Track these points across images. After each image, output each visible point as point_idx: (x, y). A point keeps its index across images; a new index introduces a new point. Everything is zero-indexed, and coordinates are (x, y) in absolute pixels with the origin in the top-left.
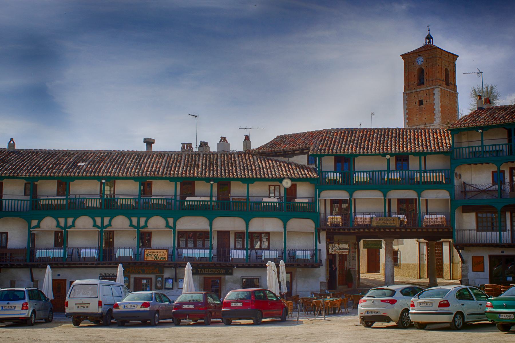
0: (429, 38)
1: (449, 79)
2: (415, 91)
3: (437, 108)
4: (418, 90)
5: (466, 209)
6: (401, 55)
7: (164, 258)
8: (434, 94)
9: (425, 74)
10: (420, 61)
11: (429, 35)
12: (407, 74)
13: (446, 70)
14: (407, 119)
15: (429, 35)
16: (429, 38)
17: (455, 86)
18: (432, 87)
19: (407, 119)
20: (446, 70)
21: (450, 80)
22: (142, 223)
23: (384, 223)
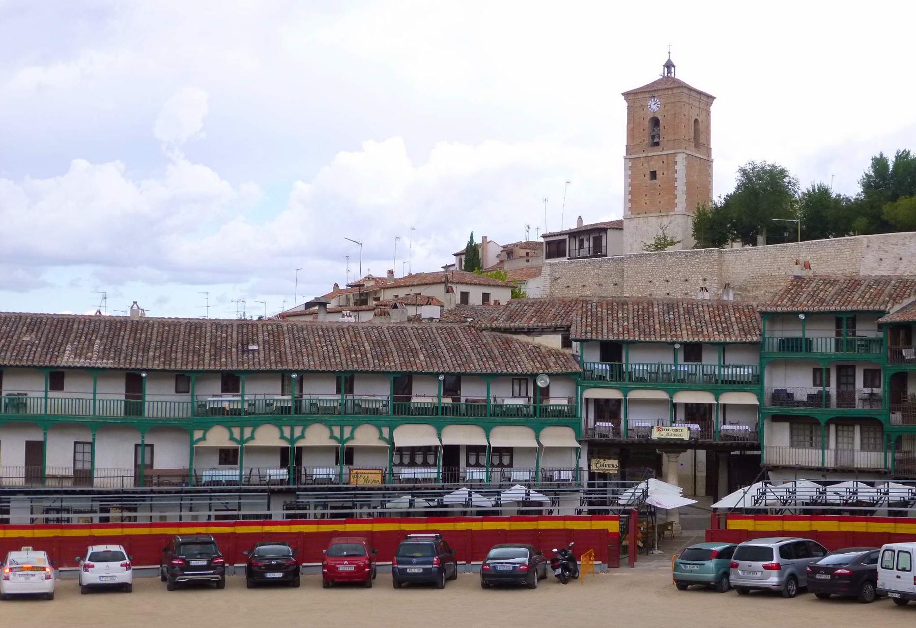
0: (669, 65)
1: (699, 137)
2: (644, 155)
3: (681, 186)
4: (650, 154)
5: (776, 418)
6: (623, 94)
7: (377, 482)
8: (676, 163)
9: (661, 127)
10: (654, 106)
11: (669, 61)
12: (632, 125)
13: (696, 121)
14: (630, 201)
15: (669, 61)
16: (669, 65)
17: (709, 150)
18: (673, 151)
19: (630, 201)
20: (696, 121)
21: (702, 138)
22: (347, 434)
23: (668, 435)
